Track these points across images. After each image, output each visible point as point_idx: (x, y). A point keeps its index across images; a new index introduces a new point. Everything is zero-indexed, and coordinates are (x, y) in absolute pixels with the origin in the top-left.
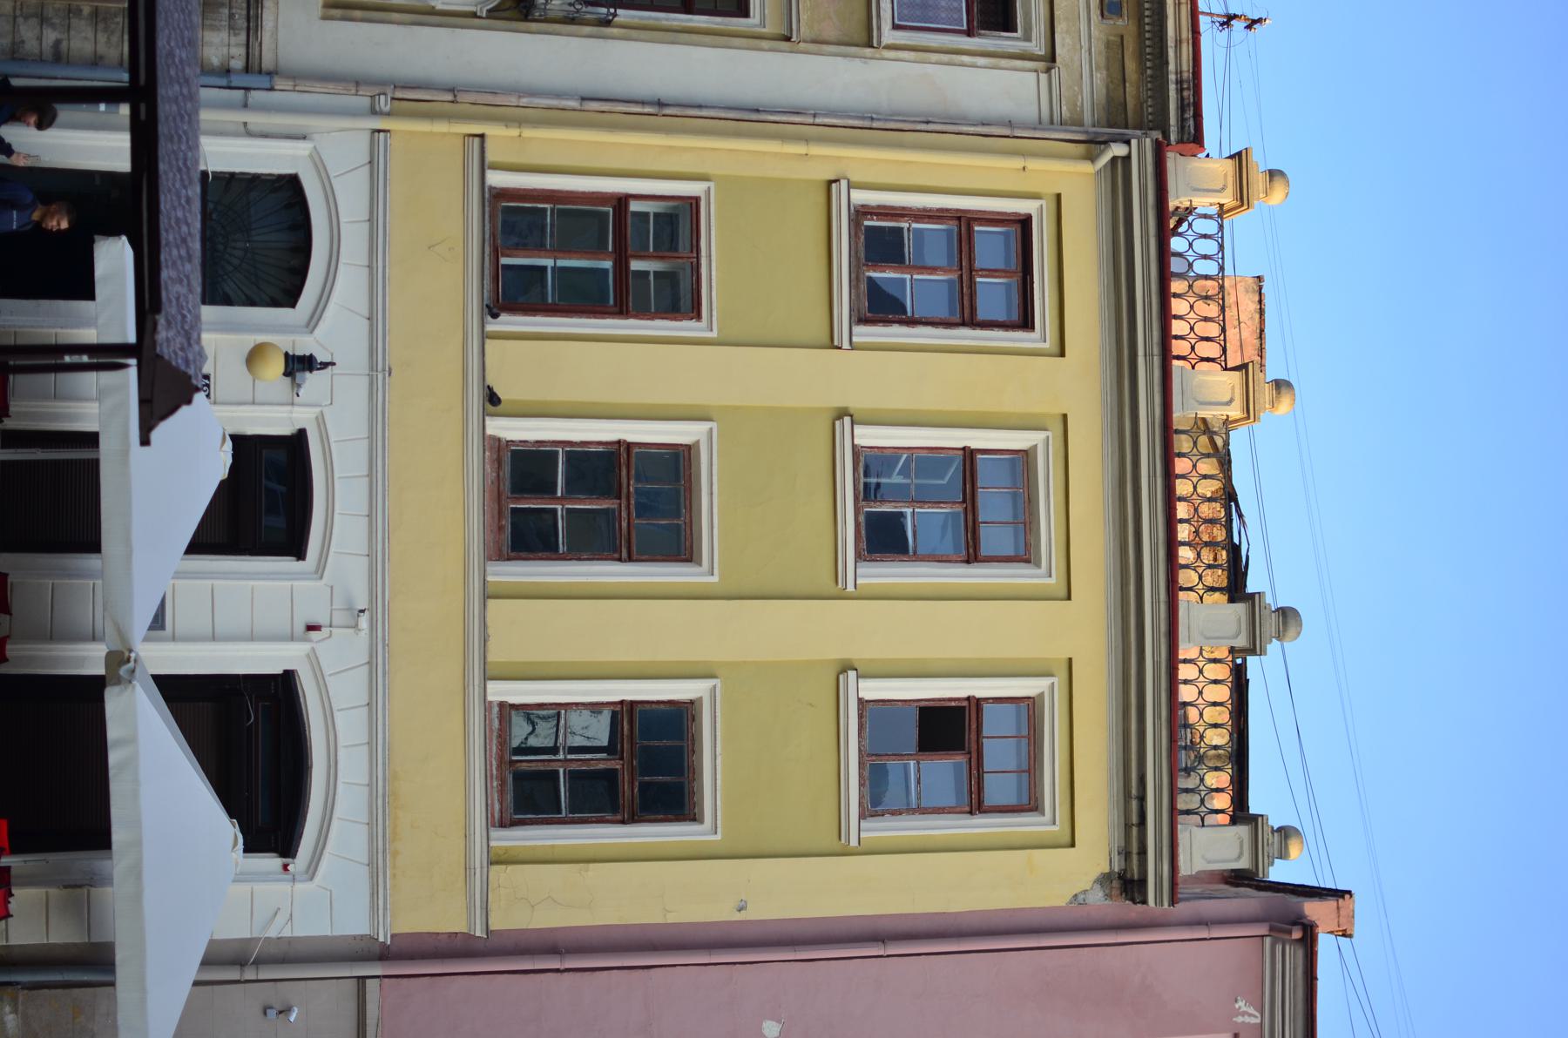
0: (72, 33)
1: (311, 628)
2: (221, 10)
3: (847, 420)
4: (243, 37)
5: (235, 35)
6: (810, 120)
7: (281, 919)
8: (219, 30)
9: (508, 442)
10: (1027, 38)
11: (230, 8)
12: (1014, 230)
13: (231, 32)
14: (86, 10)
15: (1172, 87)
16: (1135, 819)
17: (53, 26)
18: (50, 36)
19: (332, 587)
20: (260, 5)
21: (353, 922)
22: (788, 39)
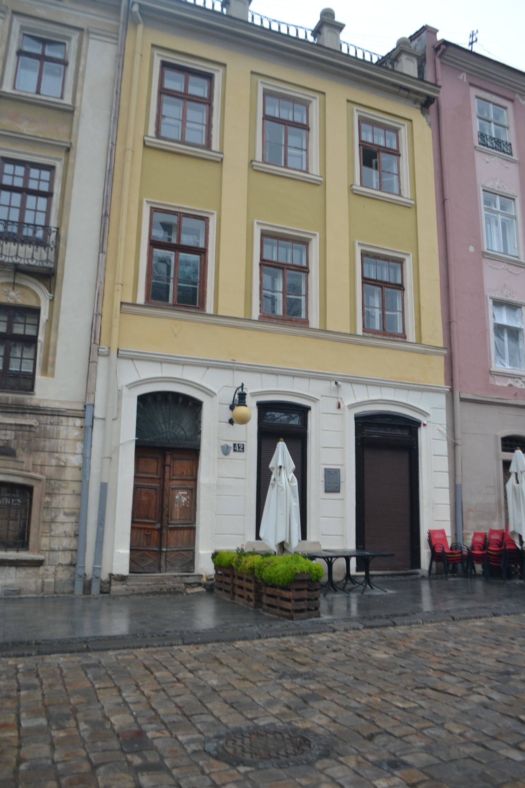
0: (60, 506)
1: (339, 407)
3: (254, 163)
4: (63, 419)
5: (62, 422)
7: (441, 429)
8: (59, 431)
9: (260, 312)
10: (69, 39)
11: (47, 424)
14: (47, 499)
16: (406, 93)
17: (56, 517)
19: (322, 396)
20: (46, 409)
21: (441, 400)
22: (68, 150)
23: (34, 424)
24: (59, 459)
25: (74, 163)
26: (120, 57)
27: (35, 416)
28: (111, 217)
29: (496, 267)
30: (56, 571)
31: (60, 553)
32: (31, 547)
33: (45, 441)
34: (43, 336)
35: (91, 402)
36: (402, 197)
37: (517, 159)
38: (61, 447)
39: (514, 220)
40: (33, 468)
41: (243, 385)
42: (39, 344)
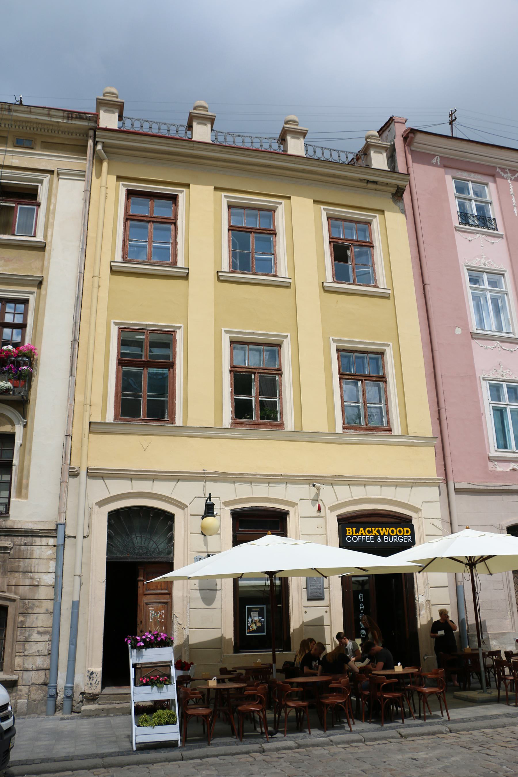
0: (33, 626)
1: (319, 509)
2: (22, 549)
3: (220, 274)
4: (37, 539)
5: (35, 543)
6: (83, 275)
9: (232, 419)
10: (41, 182)
12: (133, 199)
13: (33, 544)
14: (21, 618)
15: (70, 122)
17: (30, 636)
18: (35, 637)
19: (300, 499)
23: (8, 546)
24: (32, 578)
25: (46, 295)
26: (88, 191)
27: (10, 538)
28: (80, 341)
29: (488, 347)
30: (29, 691)
31: (34, 672)
32: (5, 668)
33: (19, 561)
34: (18, 459)
35: (62, 521)
36: (378, 288)
37: (503, 233)
38: (34, 567)
39: (505, 295)
40: (8, 589)
41: (210, 494)
42: (14, 468)
